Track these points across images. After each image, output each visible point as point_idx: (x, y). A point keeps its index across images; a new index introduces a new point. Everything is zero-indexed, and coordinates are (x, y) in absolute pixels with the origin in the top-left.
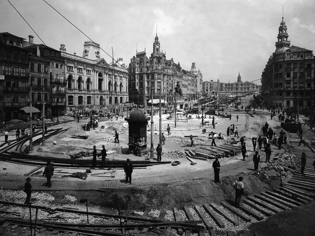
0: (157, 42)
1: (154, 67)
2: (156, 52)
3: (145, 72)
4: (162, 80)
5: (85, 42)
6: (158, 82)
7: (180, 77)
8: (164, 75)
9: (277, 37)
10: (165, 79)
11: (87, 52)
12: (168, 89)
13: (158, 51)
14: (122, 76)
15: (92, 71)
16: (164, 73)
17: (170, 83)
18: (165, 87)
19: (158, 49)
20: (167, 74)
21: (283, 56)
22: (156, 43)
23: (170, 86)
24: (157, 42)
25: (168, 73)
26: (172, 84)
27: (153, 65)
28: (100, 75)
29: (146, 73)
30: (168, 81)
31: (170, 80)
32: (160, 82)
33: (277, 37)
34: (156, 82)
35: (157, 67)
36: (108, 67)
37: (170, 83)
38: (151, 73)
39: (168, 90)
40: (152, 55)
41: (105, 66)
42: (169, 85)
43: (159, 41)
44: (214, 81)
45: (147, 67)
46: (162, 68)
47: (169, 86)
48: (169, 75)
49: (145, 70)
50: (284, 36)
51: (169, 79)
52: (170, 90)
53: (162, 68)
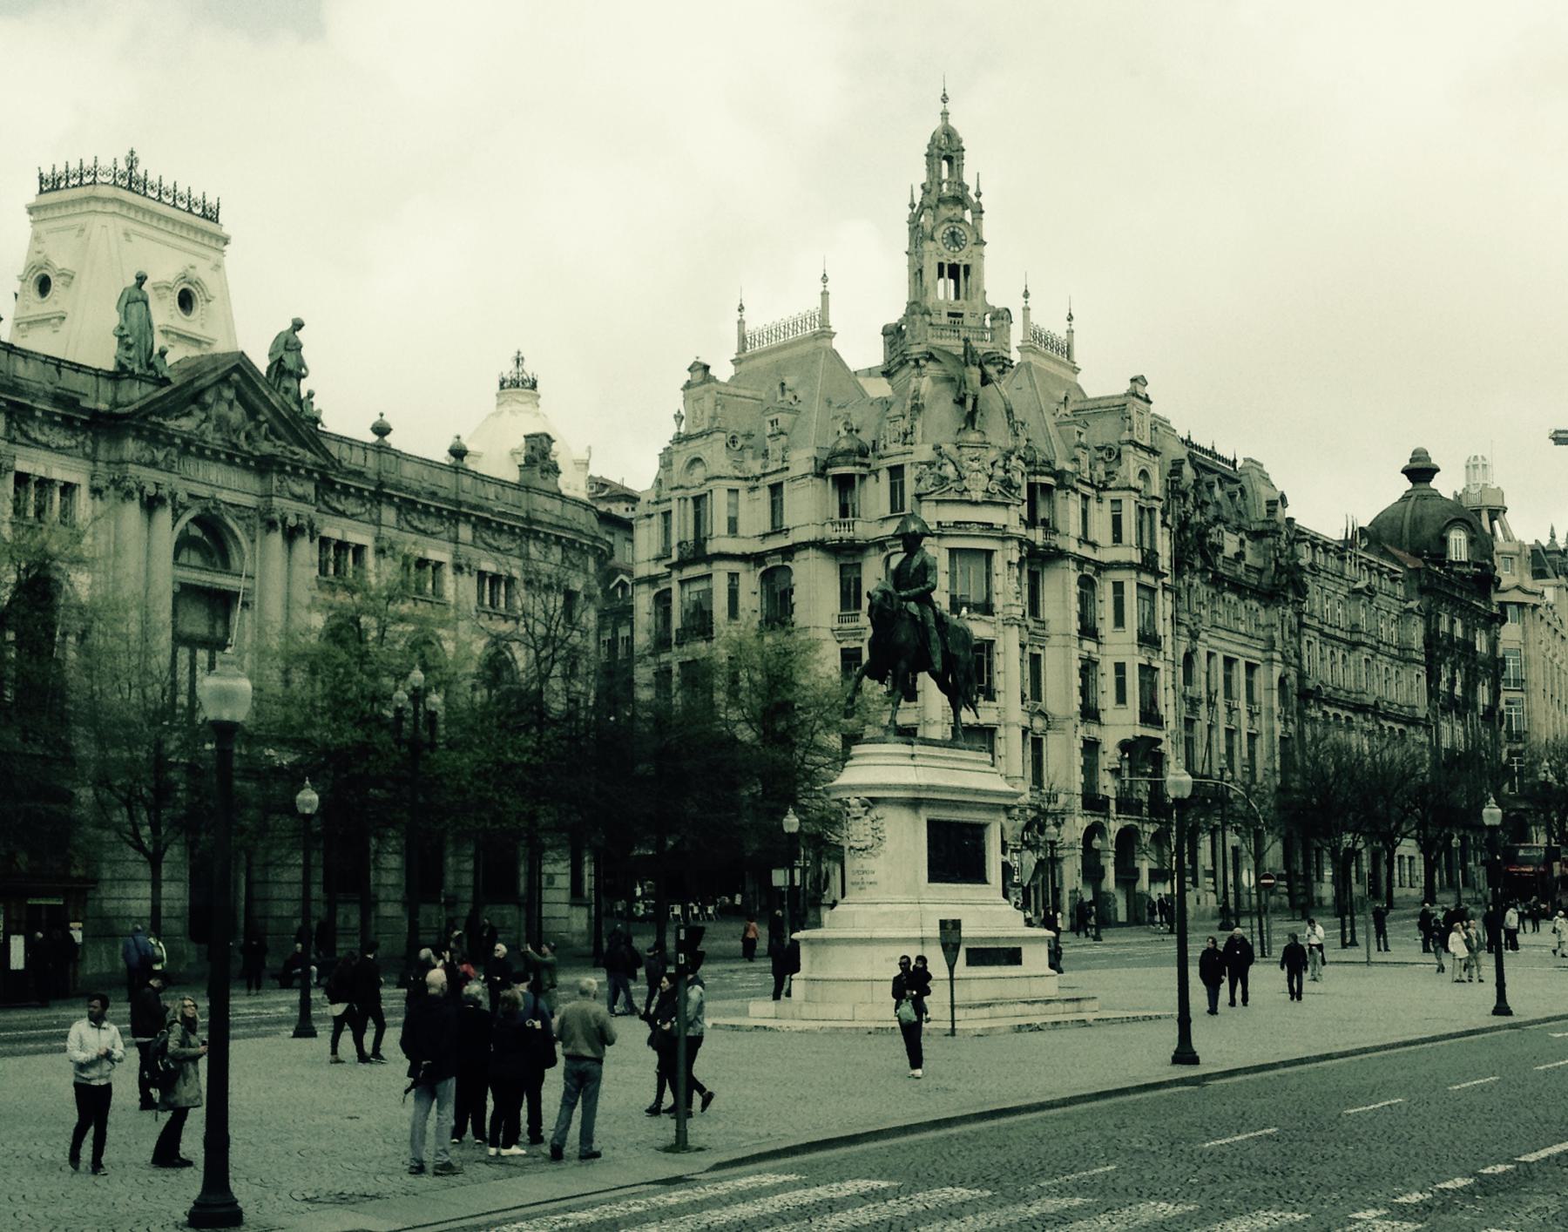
0: (946, 215)
5: (47, 172)
7: (1269, 596)
10: (1048, 610)
11: (56, 283)
12: (1094, 731)
14: (438, 552)
15: (96, 492)
16: (1038, 536)
17: (1120, 668)
19: (954, 271)
20: (1081, 562)
23: (1121, 698)
24: (946, 215)
25: (1094, 545)
26: (1147, 671)
28: (209, 536)
30: (1088, 631)
31: (1119, 621)
35: (949, 470)
37: (1120, 668)
40: (893, 334)
41: (266, 447)
42: (1107, 683)
43: (968, 178)
44: (1154, 409)
48: (1101, 567)
49: (808, 510)
51: (1105, 610)
52: (1125, 746)
53: (1008, 484)
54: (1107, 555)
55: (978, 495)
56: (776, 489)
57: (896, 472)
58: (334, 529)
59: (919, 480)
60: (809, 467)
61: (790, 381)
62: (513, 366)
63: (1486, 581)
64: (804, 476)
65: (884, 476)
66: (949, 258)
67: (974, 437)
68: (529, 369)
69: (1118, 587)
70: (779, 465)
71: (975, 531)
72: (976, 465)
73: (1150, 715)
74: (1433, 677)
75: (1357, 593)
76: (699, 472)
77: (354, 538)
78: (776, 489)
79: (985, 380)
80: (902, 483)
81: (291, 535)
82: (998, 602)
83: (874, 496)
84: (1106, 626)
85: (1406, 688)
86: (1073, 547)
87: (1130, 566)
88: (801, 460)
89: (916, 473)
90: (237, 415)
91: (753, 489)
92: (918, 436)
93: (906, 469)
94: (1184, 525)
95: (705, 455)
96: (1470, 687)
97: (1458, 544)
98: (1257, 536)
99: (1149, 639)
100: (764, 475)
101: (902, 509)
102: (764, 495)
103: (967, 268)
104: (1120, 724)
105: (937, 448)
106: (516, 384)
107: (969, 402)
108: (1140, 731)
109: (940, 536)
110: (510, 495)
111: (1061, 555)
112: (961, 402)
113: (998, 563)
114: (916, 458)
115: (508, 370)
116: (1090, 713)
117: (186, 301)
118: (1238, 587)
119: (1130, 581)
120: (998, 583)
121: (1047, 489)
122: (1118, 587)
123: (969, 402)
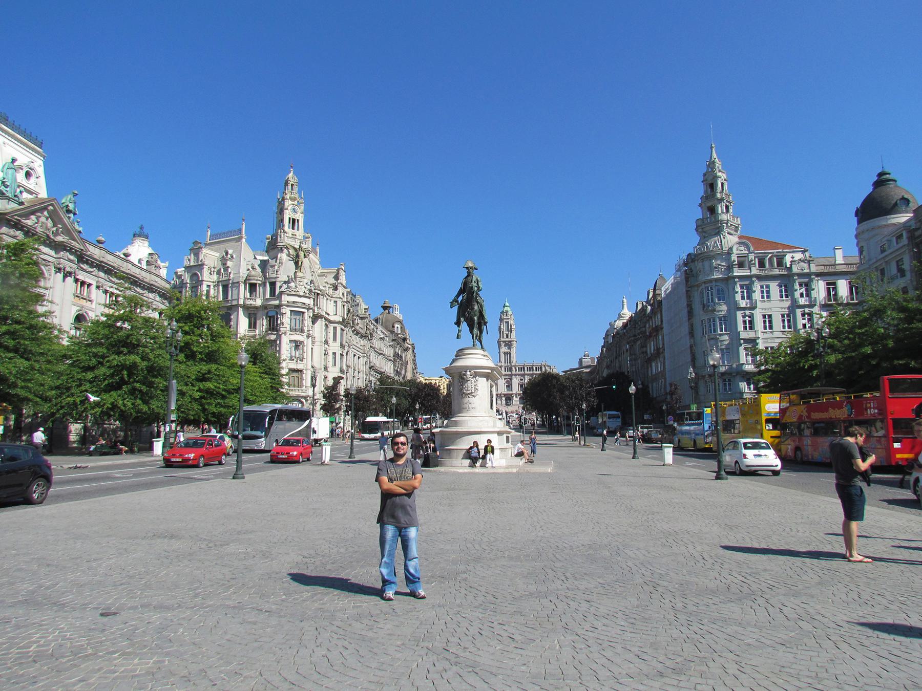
1: (278, 285)
2: (286, 228)
3: (241, 302)
4: (308, 336)
6: (291, 341)
8: (315, 318)
9: (700, 205)
13: (293, 228)
17: (334, 354)
18: (317, 365)
19: (294, 220)
20: (326, 319)
22: (288, 196)
27: (274, 276)
29: (246, 308)
30: (326, 342)
32: (301, 342)
33: (700, 205)
34: (285, 340)
36: (74, 243)
37: (334, 354)
38: (265, 307)
39: (326, 377)
41: (60, 239)
46: (310, 291)
47: (330, 364)
50: (722, 199)
51: (331, 335)
52: (334, 379)
53: (310, 291)
54: (331, 318)
55: (302, 294)
56: (225, 287)
57: (273, 285)
58: (82, 276)
59: (281, 287)
61: (230, 252)
66: (293, 216)
67: (299, 274)
69: (335, 328)
71: (300, 305)
73: (342, 371)
74: (395, 366)
75: (381, 338)
77: (88, 280)
79: (305, 256)
81: (67, 275)
82: (306, 329)
84: (331, 340)
85: (388, 369)
86: (324, 314)
87: (339, 323)
90: (50, 223)
94: (349, 311)
96: (401, 369)
98: (362, 318)
99: (342, 346)
104: (334, 372)
106: (140, 236)
108: (340, 375)
109: (287, 306)
110: (144, 274)
111: (321, 317)
113: (306, 315)
115: (137, 230)
116: (326, 369)
117: (28, 175)
118: (357, 333)
119: (339, 327)
120: (306, 322)
121: (318, 294)
122: (335, 328)
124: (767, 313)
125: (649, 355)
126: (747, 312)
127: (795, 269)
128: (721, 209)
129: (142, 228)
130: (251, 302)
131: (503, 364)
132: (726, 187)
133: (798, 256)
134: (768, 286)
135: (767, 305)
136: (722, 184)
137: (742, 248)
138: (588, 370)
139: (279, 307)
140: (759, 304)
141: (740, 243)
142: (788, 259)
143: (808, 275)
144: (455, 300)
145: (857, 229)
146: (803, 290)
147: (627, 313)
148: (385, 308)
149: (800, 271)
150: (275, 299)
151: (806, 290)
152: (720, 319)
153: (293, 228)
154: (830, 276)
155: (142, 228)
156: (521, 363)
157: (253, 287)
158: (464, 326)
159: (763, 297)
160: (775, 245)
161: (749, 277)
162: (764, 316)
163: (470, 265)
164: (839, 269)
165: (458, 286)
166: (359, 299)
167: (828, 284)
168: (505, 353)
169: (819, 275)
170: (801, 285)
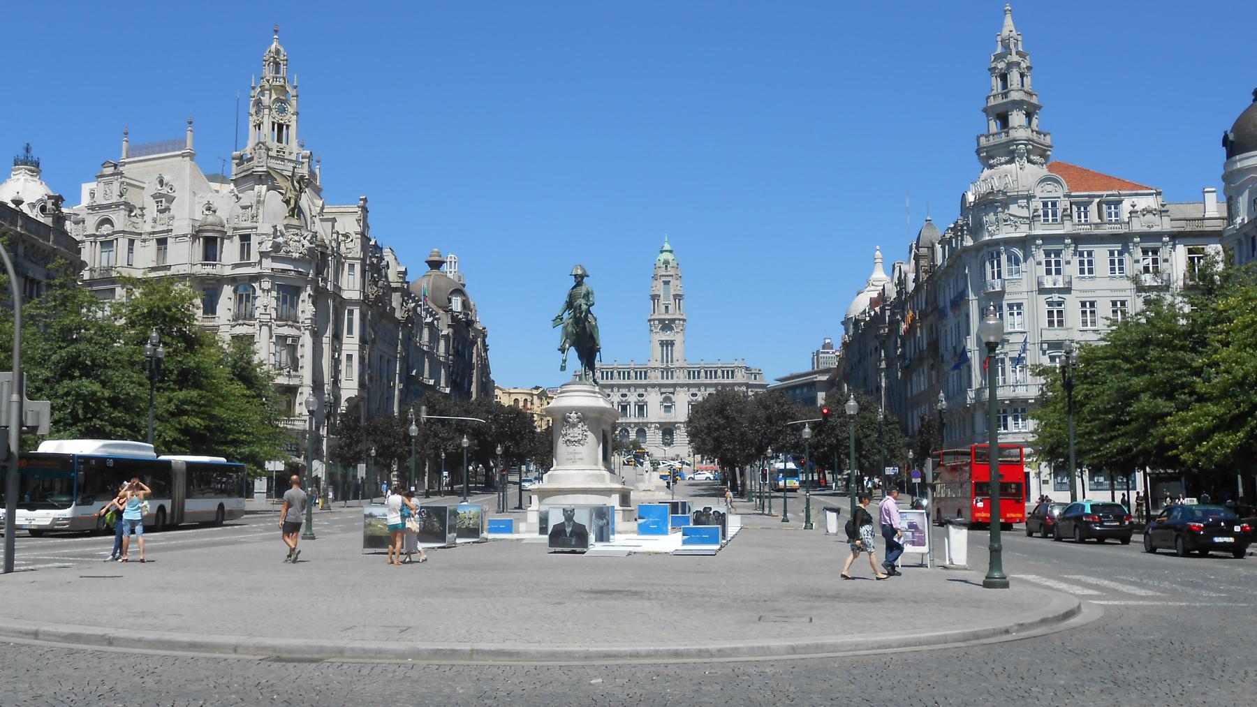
1: (254, 241)
13: (280, 140)
19: (280, 127)
21: (1025, 213)
31: (350, 331)
35: (280, 240)
37: (349, 357)
45: (207, 240)
52: (349, 400)
54: (346, 295)
56: (162, 242)
57: (245, 238)
60: (189, 230)
61: (166, 179)
62: (24, 152)
63: (470, 323)
64: (185, 236)
65: (237, 240)
66: (278, 118)
68: (34, 154)
69: (351, 312)
70: (165, 228)
72: (296, 238)
76: (106, 229)
78: (162, 242)
80: (249, 245)
82: (301, 317)
83: (230, 252)
88: (182, 226)
89: (259, 239)
91: (144, 241)
92: (260, 217)
93: (253, 237)
95: (113, 217)
97: (456, 304)
100: (154, 233)
101: (249, 258)
102: (153, 244)
103: (288, 127)
105: (275, 227)
107: (292, 202)
112: (287, 202)
114: (259, 231)
115: (21, 154)
123: (292, 202)
124: (1088, 297)
125: (907, 362)
126: (1055, 297)
127: (1137, 226)
128: (1017, 118)
129: (27, 150)
130: (208, 270)
131: (658, 364)
132: (1027, 80)
133: (1143, 203)
134: (1090, 254)
135: (1088, 284)
136: (1022, 75)
137: (1050, 188)
138: (825, 378)
139: (257, 278)
140: (1076, 284)
141: (1044, 180)
142: (1126, 205)
143: (1158, 236)
144: (560, 318)
145: (1225, 166)
146: (1150, 260)
147: (881, 280)
148: (436, 265)
149: (1146, 229)
150: (249, 265)
151: (1155, 261)
152: (1011, 306)
153: (280, 140)
154: (1192, 237)
155: (27, 150)
156: (695, 362)
157: (211, 247)
158: (572, 353)
159: (1082, 271)
160: (1108, 181)
161: (1059, 239)
162: (1083, 304)
163: (579, 272)
164: (1209, 226)
165: (565, 298)
166: (388, 257)
167: (1190, 251)
168: (663, 343)
169: (1176, 237)
170: (1145, 252)
